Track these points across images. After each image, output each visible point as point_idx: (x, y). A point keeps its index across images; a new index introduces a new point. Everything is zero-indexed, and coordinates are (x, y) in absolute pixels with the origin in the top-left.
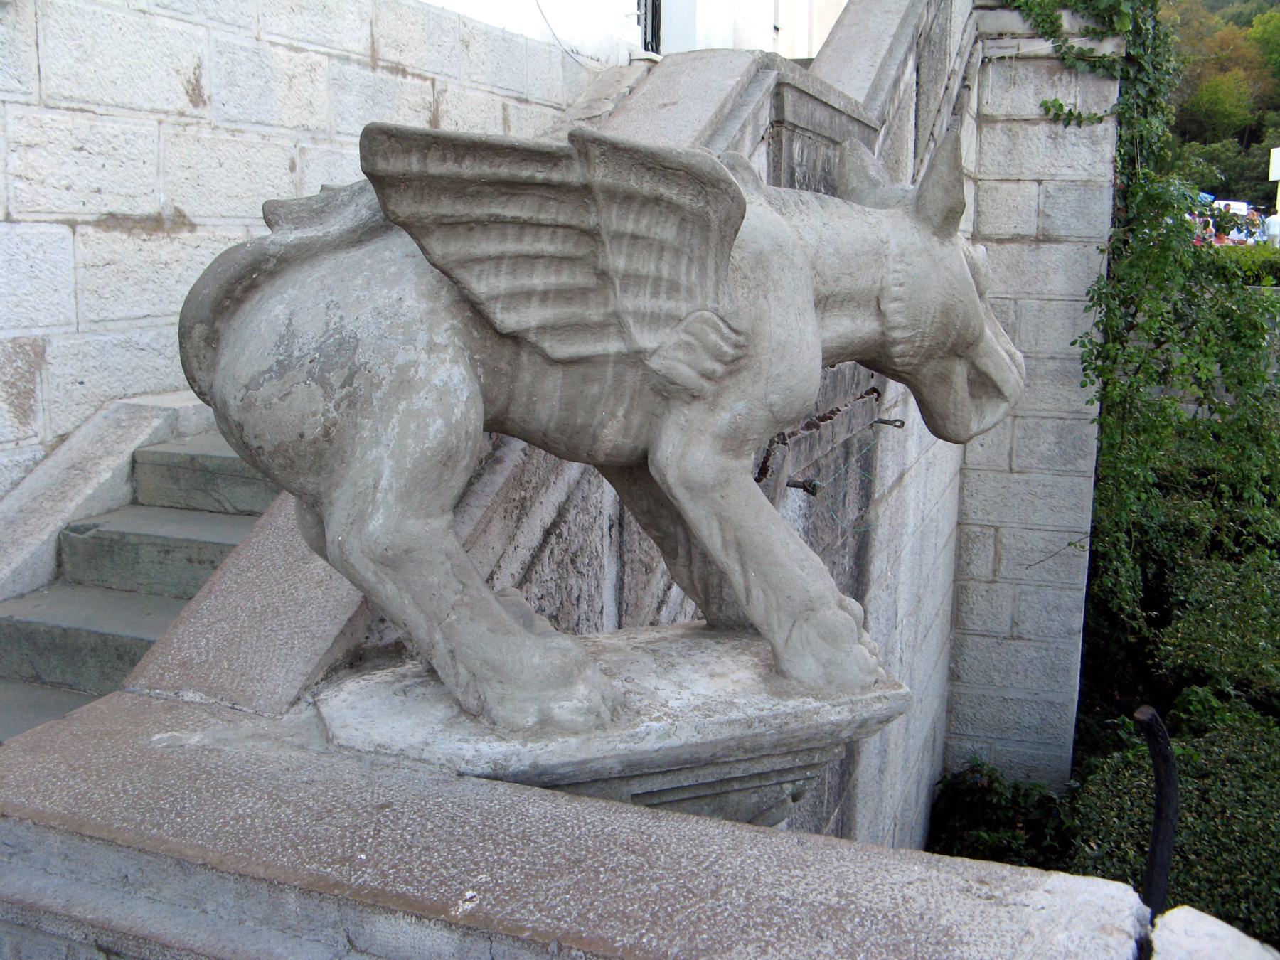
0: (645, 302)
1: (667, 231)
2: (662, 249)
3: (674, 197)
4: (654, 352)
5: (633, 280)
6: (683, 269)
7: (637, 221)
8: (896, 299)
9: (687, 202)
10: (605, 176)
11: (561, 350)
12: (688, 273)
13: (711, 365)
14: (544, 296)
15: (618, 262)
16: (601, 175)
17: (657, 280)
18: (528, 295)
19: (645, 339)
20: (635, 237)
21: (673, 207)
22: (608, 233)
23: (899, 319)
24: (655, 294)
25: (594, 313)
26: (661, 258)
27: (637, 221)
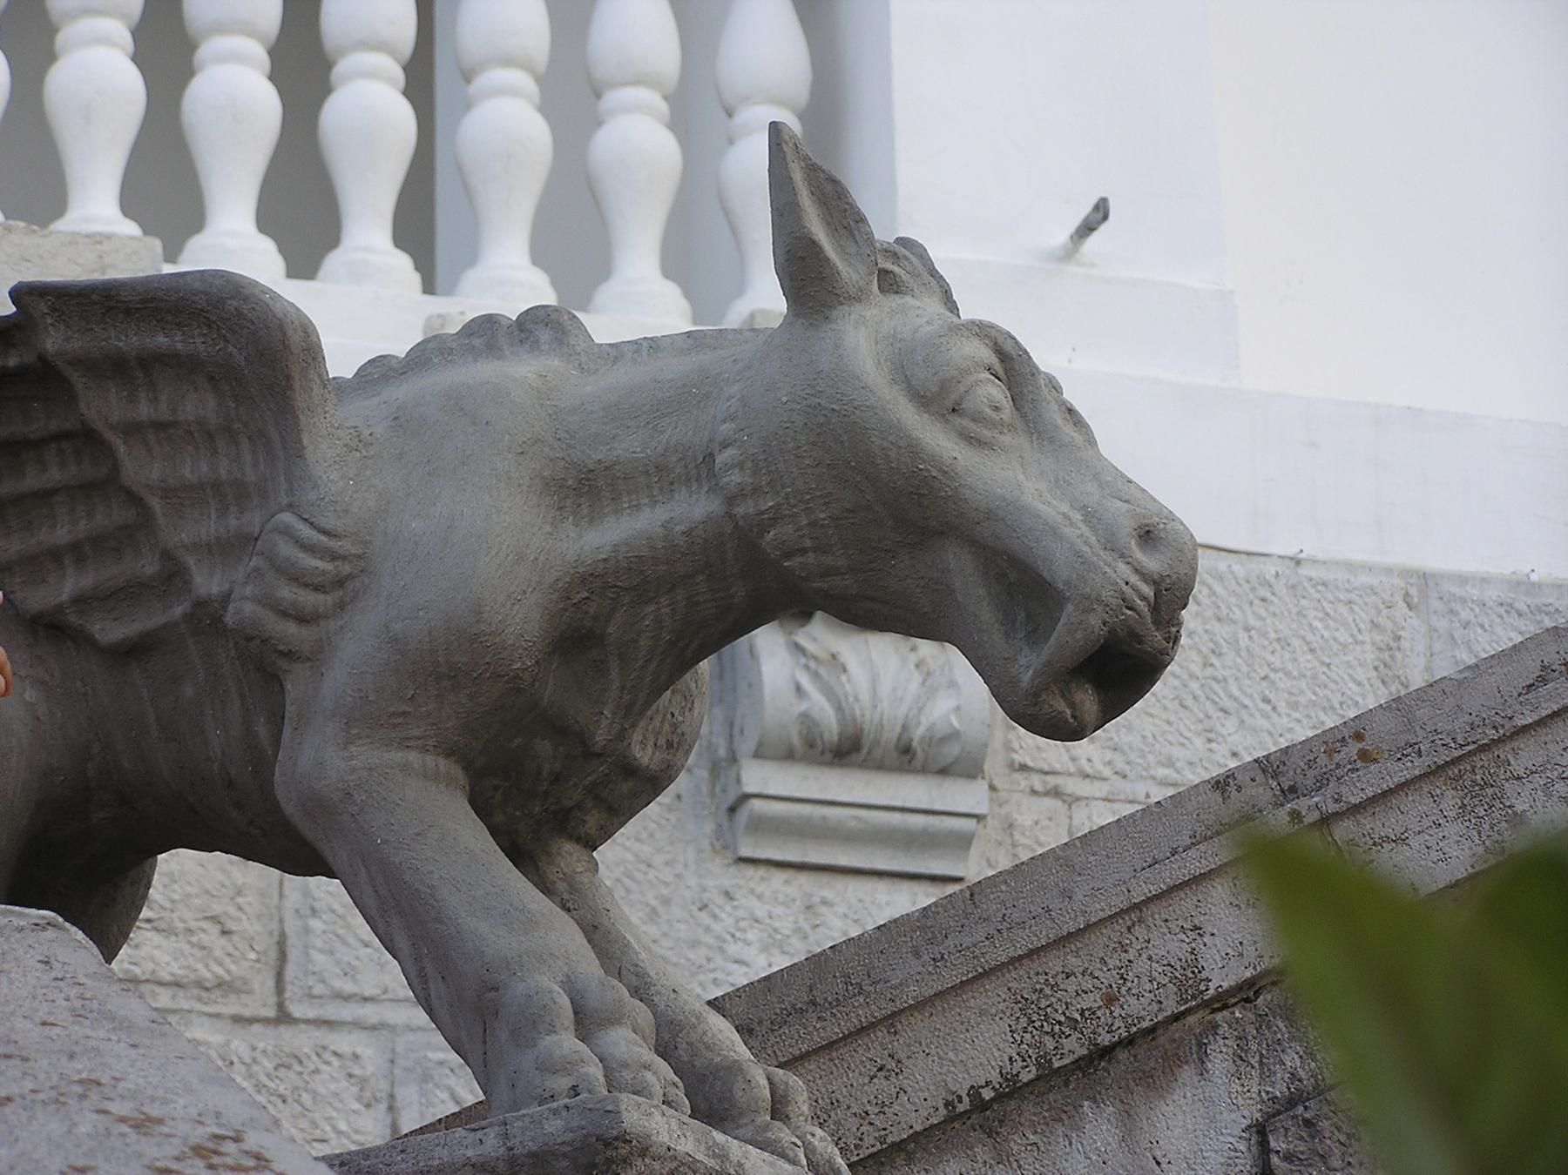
0: (208, 526)
1: (198, 405)
2: (210, 436)
3: (179, 346)
4: (226, 599)
5: (179, 495)
6: (248, 458)
7: (155, 400)
8: (725, 446)
9: (201, 348)
10: (67, 339)
11: (110, 630)
12: (256, 464)
13: (287, 593)
14: (77, 552)
15: (141, 468)
16: (53, 341)
17: (217, 486)
18: (56, 555)
19: (207, 582)
20: (159, 426)
21: (186, 367)
22: (112, 427)
23: (735, 478)
24: (223, 510)
25: (149, 567)
26: (215, 453)
27: (155, 400)
